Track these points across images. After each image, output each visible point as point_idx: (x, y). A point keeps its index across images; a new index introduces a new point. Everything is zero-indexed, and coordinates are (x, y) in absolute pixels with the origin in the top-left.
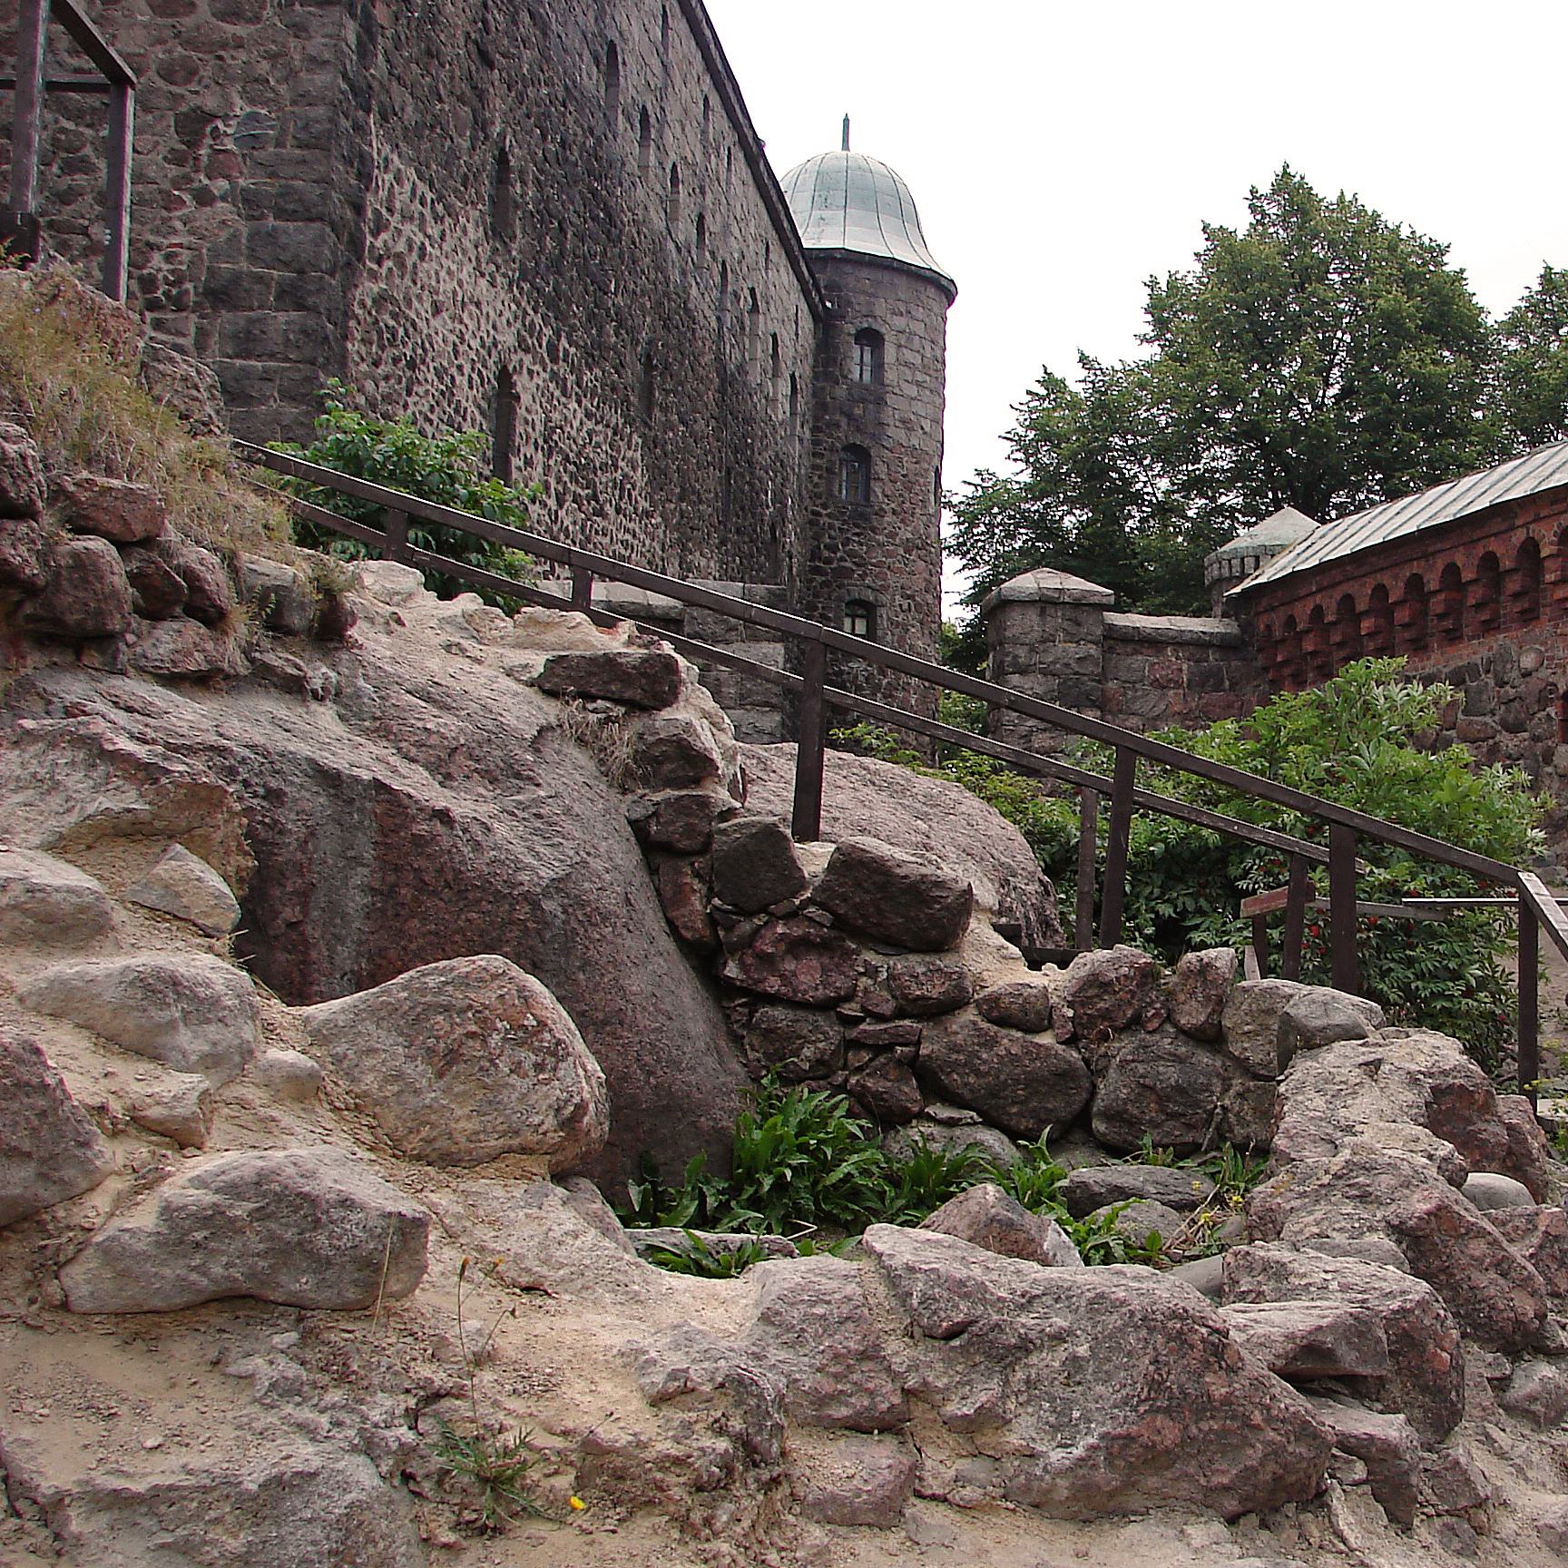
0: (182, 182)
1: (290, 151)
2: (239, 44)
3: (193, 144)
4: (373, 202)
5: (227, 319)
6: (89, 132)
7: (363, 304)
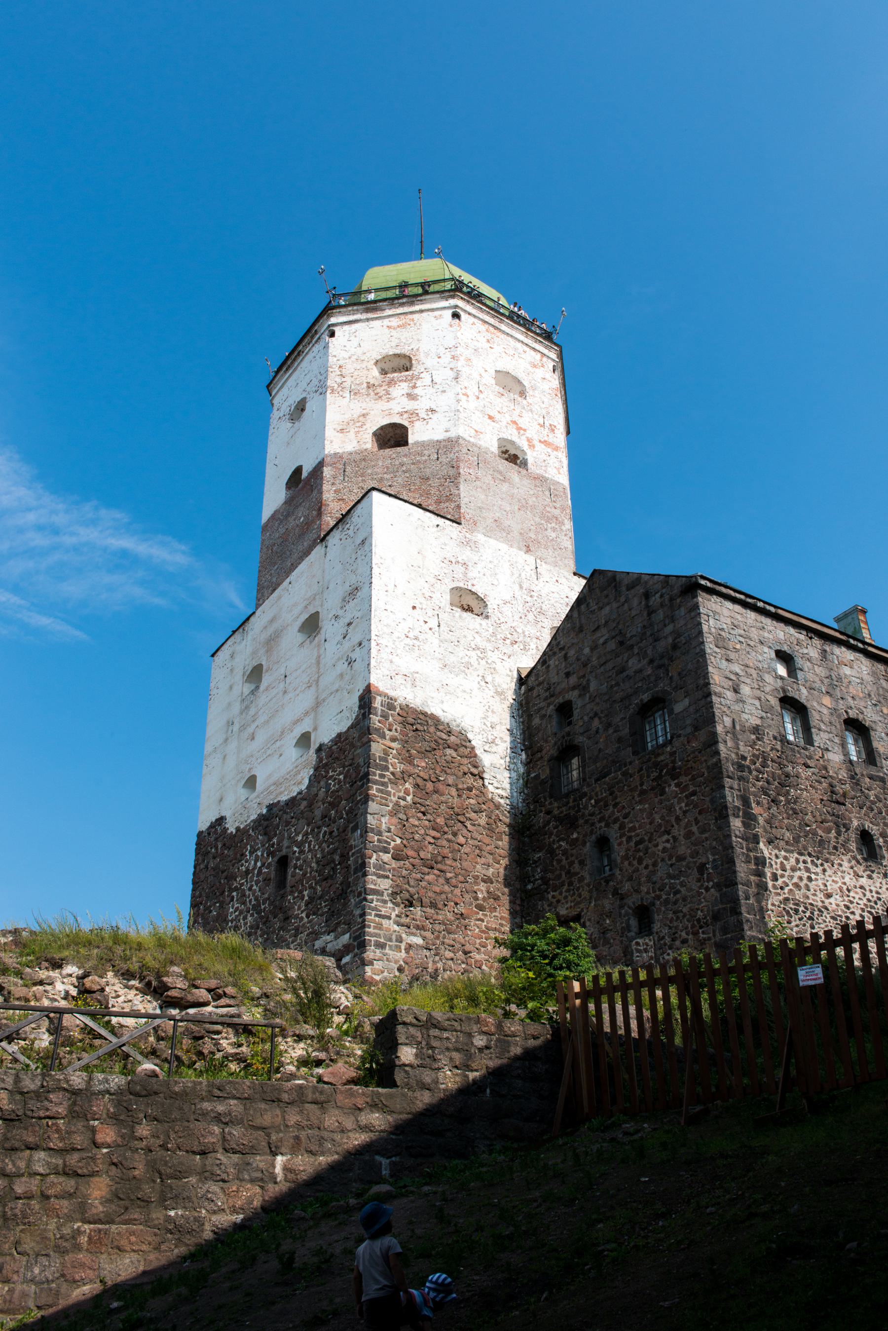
0: (701, 887)
1: (726, 866)
3: (702, 874)
4: (768, 872)
5: (719, 925)
6: (678, 881)
7: (773, 905)
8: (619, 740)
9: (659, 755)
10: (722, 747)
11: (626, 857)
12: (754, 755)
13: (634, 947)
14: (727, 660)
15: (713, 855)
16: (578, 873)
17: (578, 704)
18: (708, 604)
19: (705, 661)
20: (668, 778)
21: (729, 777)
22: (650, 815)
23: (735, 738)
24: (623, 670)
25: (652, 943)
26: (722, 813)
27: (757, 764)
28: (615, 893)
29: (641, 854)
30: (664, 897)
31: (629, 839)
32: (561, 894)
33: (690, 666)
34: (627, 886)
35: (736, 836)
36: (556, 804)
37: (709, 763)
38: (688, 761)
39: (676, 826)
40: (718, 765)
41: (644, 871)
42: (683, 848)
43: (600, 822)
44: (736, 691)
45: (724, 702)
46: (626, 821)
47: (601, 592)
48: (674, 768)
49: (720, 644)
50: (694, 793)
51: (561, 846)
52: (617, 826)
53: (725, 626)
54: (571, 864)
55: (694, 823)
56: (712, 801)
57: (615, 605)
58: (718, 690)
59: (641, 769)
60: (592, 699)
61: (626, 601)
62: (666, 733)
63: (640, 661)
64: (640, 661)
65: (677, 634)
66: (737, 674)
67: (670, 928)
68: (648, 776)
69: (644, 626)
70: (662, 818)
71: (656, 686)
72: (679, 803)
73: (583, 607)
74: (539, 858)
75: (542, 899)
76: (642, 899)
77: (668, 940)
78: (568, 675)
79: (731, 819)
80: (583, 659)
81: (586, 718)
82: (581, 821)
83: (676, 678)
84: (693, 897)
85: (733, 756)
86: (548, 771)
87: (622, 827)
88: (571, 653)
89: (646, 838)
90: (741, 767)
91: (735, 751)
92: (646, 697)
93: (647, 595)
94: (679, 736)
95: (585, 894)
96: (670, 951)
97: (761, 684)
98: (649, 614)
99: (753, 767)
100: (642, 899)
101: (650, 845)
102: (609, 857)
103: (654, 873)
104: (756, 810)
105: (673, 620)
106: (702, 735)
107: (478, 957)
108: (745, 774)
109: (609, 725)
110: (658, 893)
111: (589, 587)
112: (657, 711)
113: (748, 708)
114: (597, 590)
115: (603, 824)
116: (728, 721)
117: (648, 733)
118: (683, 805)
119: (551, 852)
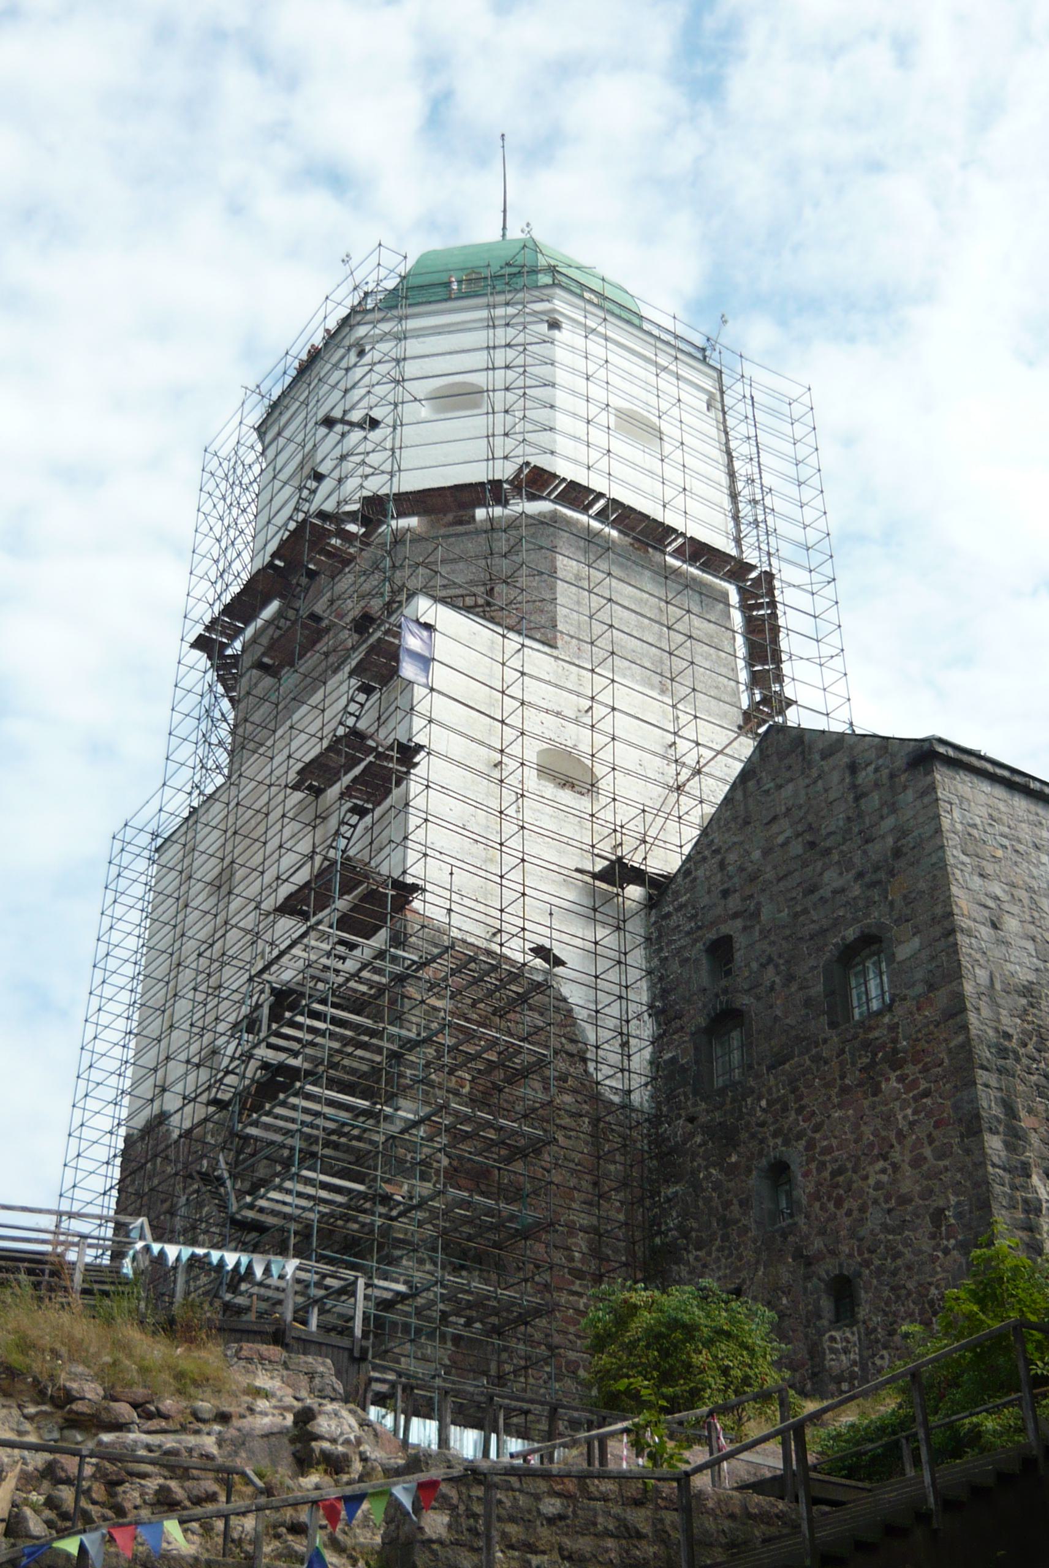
2: (946, 1169)
3: (939, 1227)
8: (808, 1003)
9: (871, 1029)
10: (972, 1017)
11: (816, 1196)
12: (1024, 1032)
13: (826, 1344)
14: (981, 875)
15: (956, 1194)
16: (738, 1221)
17: (741, 941)
18: (951, 786)
19: (946, 876)
20: (885, 1067)
21: (983, 1068)
22: (856, 1126)
23: (995, 1004)
24: (811, 890)
25: (855, 1338)
26: (972, 1126)
27: (1030, 1047)
28: (798, 1255)
29: (841, 1192)
30: (877, 1262)
31: (822, 1165)
32: (709, 1254)
33: (922, 885)
34: (818, 1244)
35: (994, 1165)
36: (703, 1105)
37: (952, 1045)
38: (919, 1040)
39: (898, 1147)
40: (967, 1047)
41: (845, 1219)
42: (908, 1182)
43: (775, 1135)
44: (995, 926)
45: (975, 943)
46: (818, 1136)
47: (780, 760)
48: (895, 1051)
49: (970, 849)
50: (927, 1094)
51: (711, 1175)
52: (801, 1145)
53: (978, 821)
54: (727, 1204)
55: (926, 1144)
56: (956, 1107)
57: (802, 782)
58: (965, 923)
59: (843, 1051)
60: (765, 934)
61: (819, 777)
62: (883, 993)
63: (841, 874)
64: (841, 874)
65: (902, 832)
66: (997, 898)
67: (886, 1314)
68: (853, 1064)
69: (849, 819)
70: (876, 1133)
71: (867, 915)
72: (902, 1109)
73: (751, 784)
74: (676, 1193)
75: (679, 1261)
76: (841, 1265)
77: (881, 1333)
78: (725, 894)
79: (987, 1136)
80: (750, 868)
81: (754, 965)
82: (744, 1136)
83: (899, 903)
84: (923, 1263)
85: (991, 1032)
86: (692, 1052)
87: (811, 1146)
88: (732, 857)
89: (849, 1165)
90: (1003, 1052)
91: (994, 1024)
92: (851, 933)
93: (853, 768)
94: (904, 999)
95: (749, 1255)
96: (885, 1353)
97: (1036, 915)
98: (857, 799)
99: (1022, 1051)
100: (841, 1265)
101: (855, 1177)
102: (789, 1194)
103: (861, 1221)
104: (1026, 1122)
105: (894, 809)
106: (941, 997)
107: (572, 1355)
108: (1010, 1062)
109: (790, 978)
110: (866, 1256)
111: (761, 751)
112: (869, 957)
113: (1014, 954)
114: (774, 758)
115: (779, 1141)
116: (982, 975)
117: (854, 992)
118: (909, 1111)
119: (696, 1187)
